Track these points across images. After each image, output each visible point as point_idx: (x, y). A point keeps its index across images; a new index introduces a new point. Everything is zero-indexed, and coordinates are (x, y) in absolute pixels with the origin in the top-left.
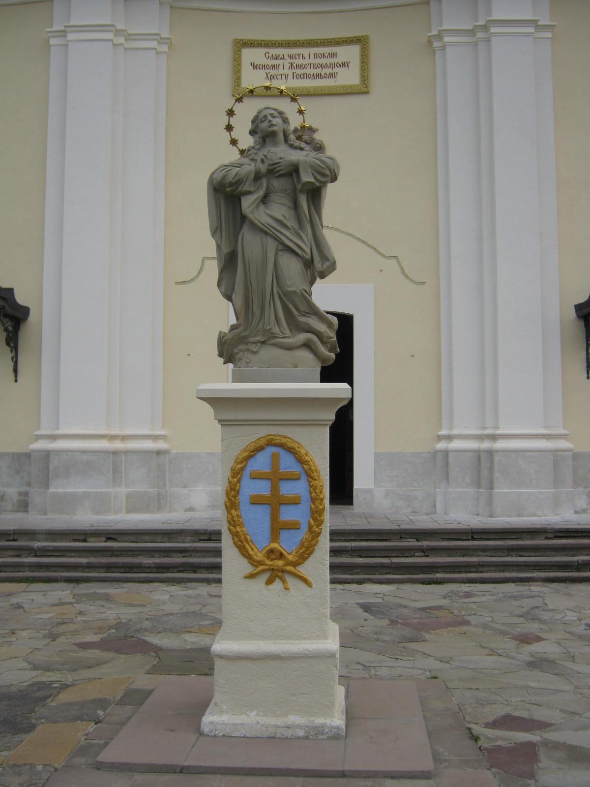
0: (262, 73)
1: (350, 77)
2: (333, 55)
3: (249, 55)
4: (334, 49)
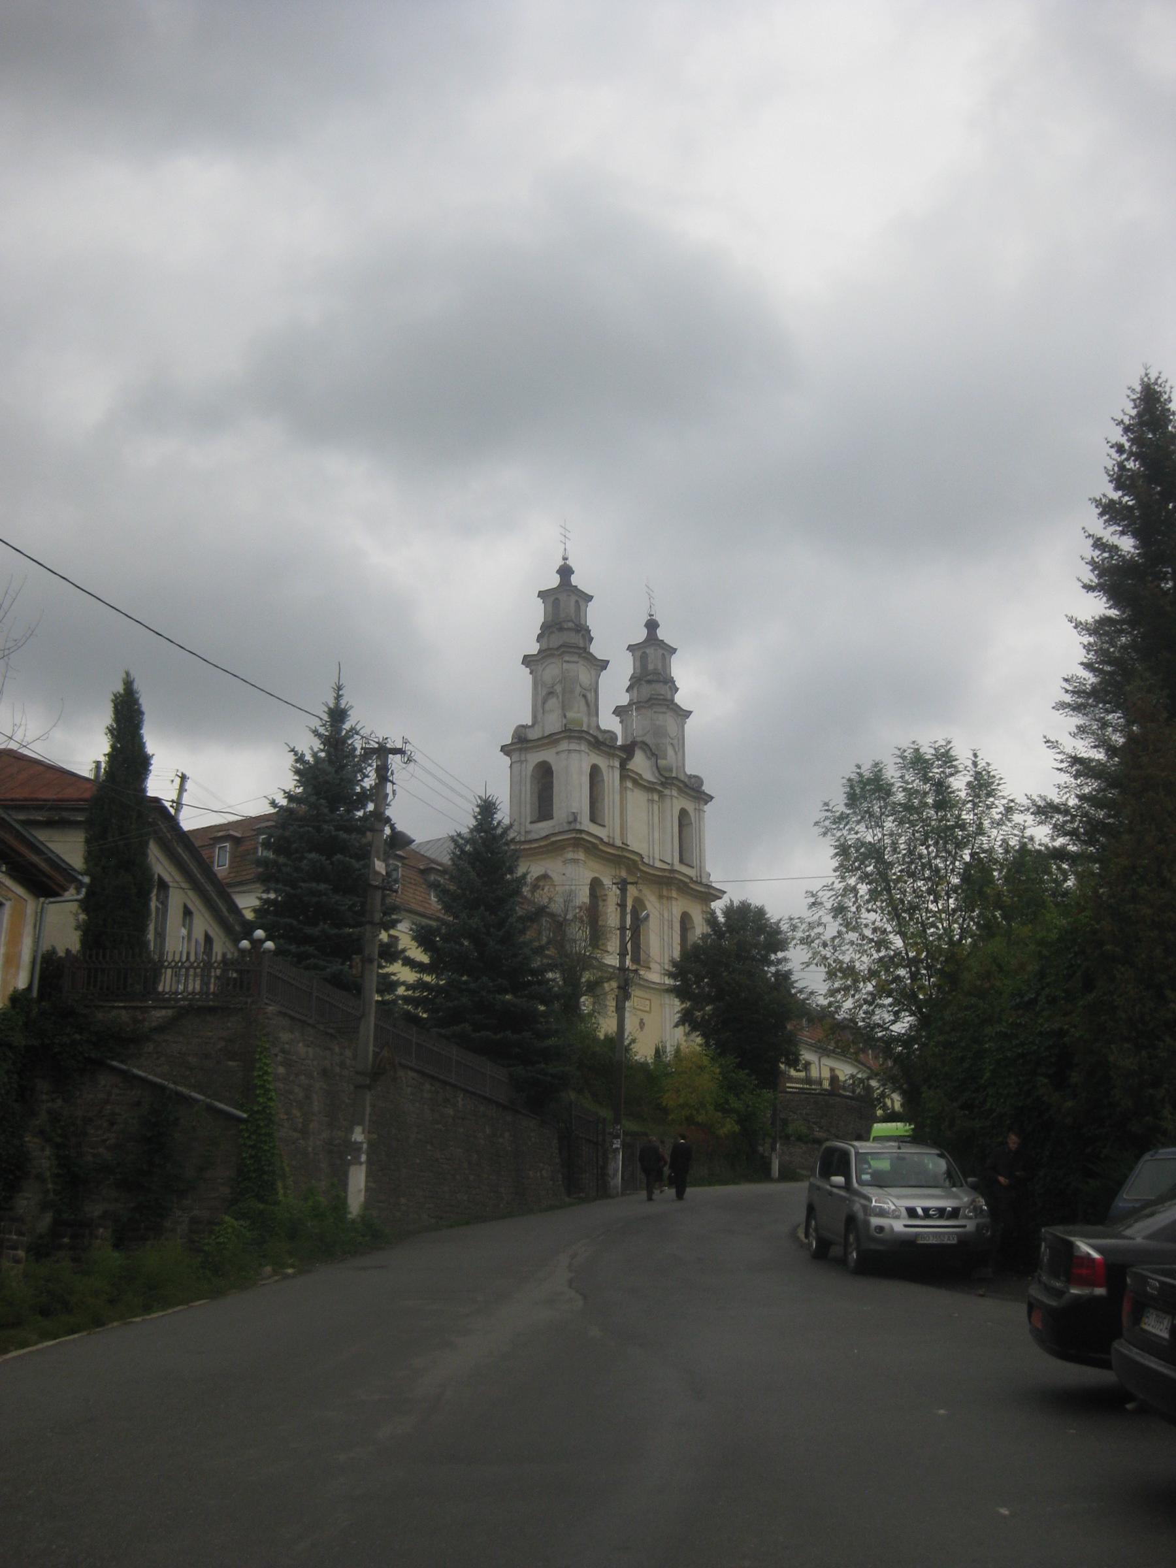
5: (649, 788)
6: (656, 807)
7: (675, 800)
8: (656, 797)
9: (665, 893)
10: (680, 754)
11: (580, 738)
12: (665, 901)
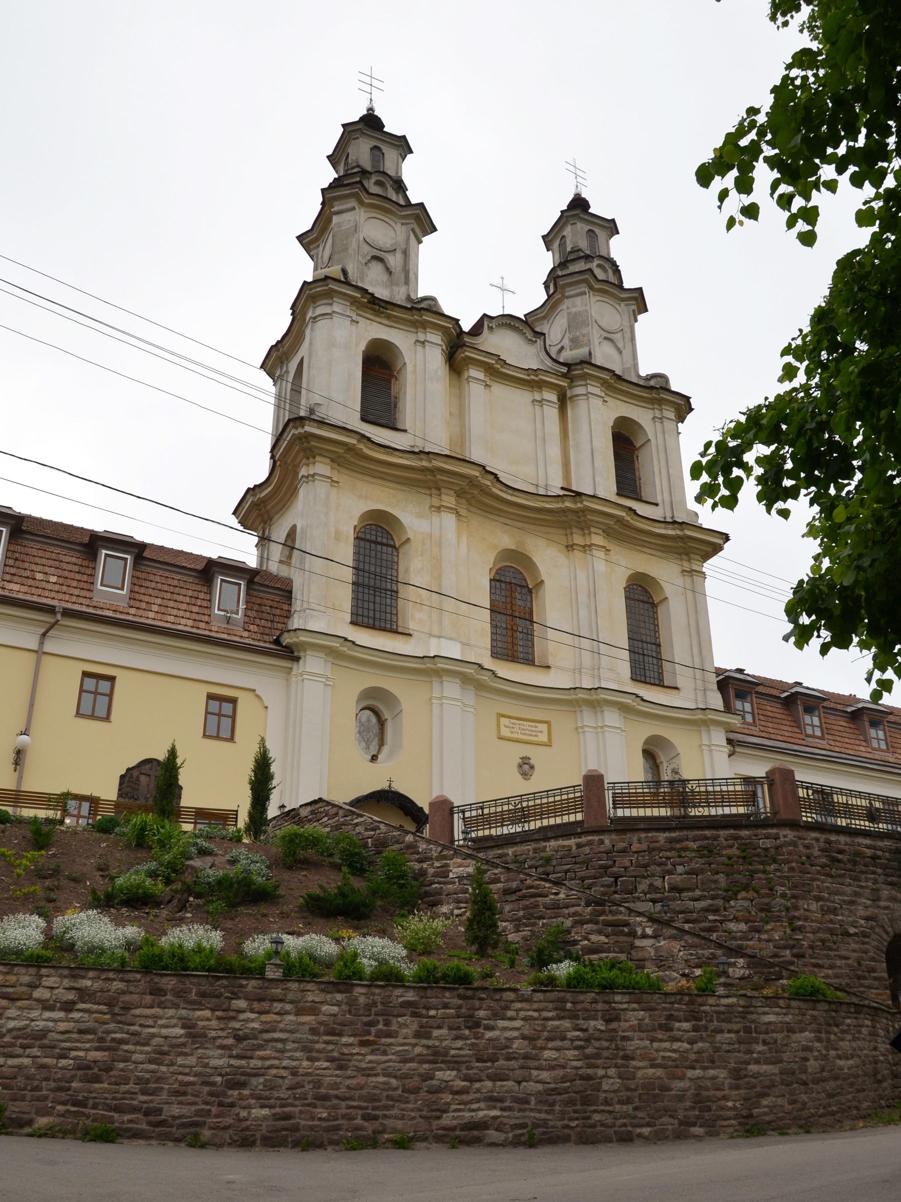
0: (508, 730)
1: (543, 738)
2: (536, 727)
3: (503, 721)
4: (537, 724)
5: (531, 381)
6: (552, 413)
7: (596, 402)
8: (553, 397)
9: (578, 539)
10: (627, 352)
11: (329, 295)
12: (578, 554)
